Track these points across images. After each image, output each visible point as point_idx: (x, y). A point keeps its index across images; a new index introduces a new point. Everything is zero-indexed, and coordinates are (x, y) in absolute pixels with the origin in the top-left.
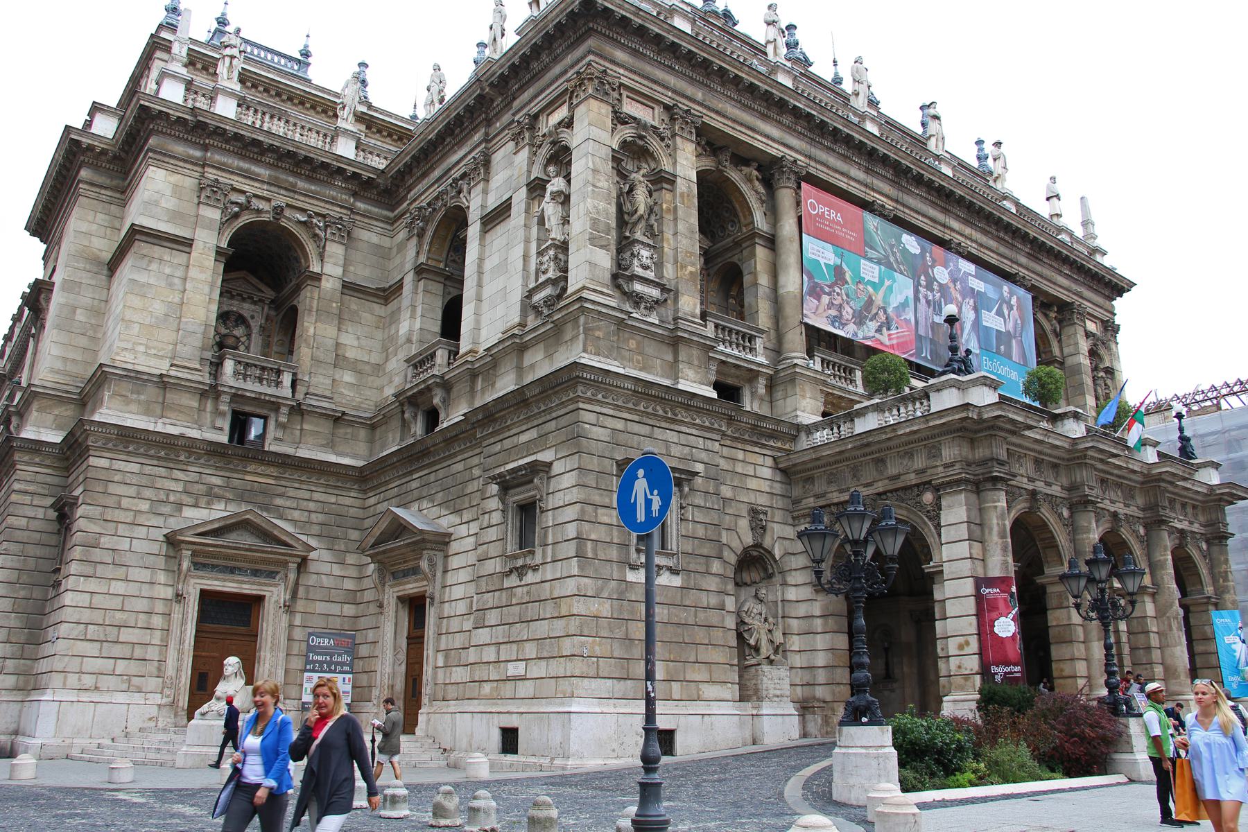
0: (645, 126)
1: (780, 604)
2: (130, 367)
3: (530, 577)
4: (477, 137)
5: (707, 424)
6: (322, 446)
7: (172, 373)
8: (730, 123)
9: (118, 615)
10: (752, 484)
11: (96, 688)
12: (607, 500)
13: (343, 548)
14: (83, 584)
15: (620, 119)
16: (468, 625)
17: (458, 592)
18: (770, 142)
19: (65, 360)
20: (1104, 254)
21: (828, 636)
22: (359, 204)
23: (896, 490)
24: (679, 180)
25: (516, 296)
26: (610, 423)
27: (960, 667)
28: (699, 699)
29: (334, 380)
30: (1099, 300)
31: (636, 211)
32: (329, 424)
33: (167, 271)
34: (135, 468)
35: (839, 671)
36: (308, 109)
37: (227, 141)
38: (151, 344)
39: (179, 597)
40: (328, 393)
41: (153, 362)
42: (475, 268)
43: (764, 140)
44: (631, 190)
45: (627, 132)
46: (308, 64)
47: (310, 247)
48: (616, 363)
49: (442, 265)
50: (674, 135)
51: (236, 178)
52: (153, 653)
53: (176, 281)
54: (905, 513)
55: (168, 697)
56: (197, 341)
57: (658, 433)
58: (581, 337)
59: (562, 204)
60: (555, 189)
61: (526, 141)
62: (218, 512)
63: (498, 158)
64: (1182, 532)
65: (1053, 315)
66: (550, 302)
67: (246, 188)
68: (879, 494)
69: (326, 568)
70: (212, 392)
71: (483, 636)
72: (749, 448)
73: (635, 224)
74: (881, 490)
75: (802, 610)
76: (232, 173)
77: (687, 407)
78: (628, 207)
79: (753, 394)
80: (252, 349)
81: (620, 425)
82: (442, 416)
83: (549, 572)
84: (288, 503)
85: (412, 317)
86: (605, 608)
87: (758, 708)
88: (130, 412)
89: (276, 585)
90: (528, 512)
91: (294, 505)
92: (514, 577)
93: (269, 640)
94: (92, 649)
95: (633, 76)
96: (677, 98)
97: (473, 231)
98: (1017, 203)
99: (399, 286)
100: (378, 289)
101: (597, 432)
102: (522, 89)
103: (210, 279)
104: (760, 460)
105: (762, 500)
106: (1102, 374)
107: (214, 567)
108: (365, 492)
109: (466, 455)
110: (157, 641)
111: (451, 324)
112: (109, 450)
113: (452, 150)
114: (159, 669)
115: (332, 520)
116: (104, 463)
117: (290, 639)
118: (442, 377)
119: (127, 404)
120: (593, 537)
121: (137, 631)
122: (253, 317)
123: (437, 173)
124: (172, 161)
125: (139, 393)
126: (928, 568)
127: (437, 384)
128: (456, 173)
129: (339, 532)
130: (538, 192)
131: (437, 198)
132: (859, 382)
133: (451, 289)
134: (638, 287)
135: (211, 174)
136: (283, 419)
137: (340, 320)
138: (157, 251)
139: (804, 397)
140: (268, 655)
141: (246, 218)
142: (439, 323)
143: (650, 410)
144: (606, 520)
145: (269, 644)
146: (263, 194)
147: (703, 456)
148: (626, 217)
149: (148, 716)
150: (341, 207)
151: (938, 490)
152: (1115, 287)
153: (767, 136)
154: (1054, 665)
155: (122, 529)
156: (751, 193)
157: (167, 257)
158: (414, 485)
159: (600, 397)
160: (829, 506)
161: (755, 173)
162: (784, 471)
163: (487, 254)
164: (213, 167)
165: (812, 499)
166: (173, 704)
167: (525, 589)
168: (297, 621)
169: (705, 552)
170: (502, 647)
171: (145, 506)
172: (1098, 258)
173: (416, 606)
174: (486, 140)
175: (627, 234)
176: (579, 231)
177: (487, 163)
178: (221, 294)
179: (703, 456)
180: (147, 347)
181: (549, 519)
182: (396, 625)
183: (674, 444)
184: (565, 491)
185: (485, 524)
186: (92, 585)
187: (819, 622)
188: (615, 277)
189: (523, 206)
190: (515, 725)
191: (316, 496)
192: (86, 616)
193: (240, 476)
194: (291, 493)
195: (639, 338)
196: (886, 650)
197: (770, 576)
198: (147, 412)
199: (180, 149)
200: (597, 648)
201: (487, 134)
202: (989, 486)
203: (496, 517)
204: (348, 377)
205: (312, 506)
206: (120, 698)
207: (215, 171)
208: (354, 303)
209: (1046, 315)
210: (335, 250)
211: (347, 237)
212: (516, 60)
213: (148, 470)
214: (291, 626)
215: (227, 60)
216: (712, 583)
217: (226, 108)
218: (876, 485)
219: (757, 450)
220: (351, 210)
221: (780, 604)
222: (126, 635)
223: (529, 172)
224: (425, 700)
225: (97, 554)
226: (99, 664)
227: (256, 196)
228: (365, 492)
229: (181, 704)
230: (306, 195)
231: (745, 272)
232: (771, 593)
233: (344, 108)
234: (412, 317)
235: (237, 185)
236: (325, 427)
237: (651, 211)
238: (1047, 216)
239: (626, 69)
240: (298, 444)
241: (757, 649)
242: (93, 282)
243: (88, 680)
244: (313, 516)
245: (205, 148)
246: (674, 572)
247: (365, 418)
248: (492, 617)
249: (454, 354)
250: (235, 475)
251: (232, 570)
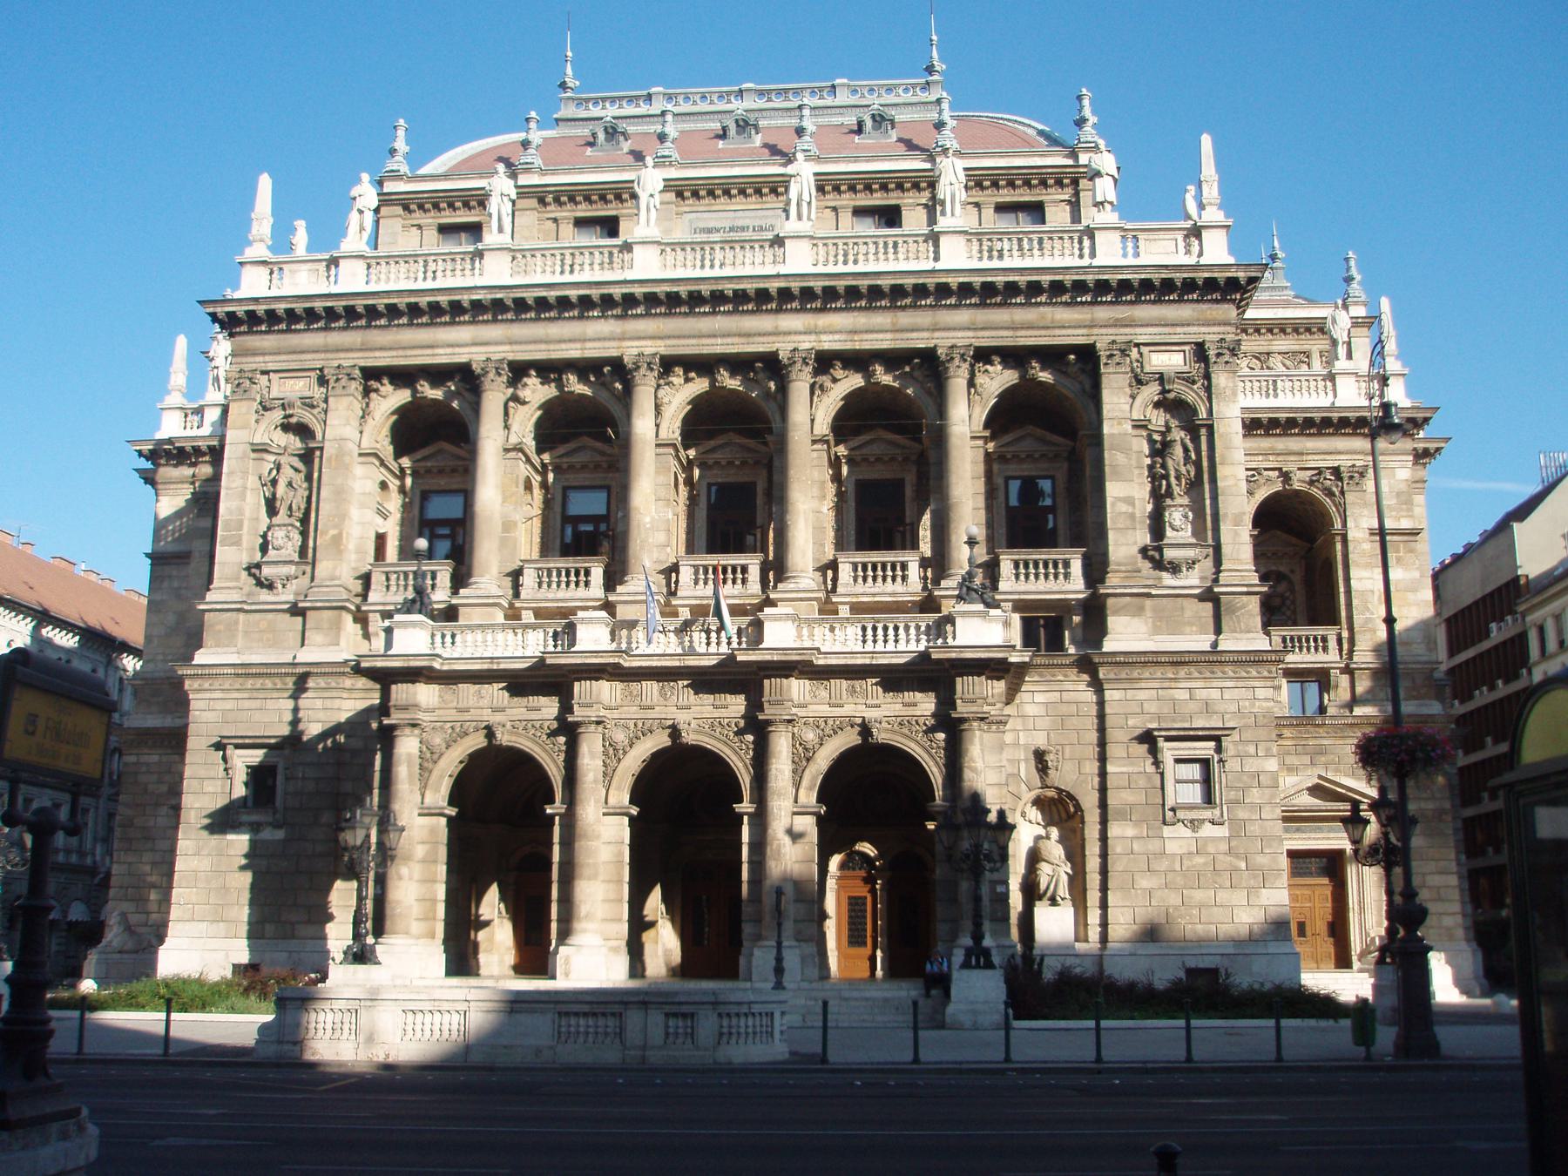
0: (292, 405)
5: (323, 685)
8: (401, 353)
12: (212, 774)
18: (457, 350)
24: (327, 445)
26: (220, 705)
28: (293, 937)
33: (176, 584)
34: (155, 758)
43: (449, 350)
57: (270, 704)
81: (229, 705)
86: (204, 864)
116: (132, 759)
134: (267, 571)
144: (210, 789)
157: (174, 573)
213: (164, 759)
246: (277, 826)
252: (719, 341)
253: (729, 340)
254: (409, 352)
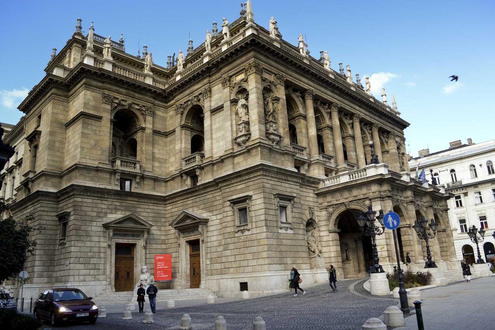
1: (318, 237)
2: (85, 164)
3: (247, 233)
4: (206, 81)
5: (296, 181)
6: (151, 189)
7: (100, 166)
9: (90, 254)
10: (308, 199)
11: (85, 281)
12: (272, 207)
13: (160, 225)
14: (77, 244)
15: (264, 80)
16: (221, 249)
17: (214, 238)
18: (305, 84)
19: (53, 161)
20: (399, 114)
21: (335, 247)
22: (157, 102)
23: (356, 200)
24: (281, 99)
25: (229, 139)
27: (381, 255)
29: (153, 166)
30: (399, 130)
31: (270, 111)
33: (94, 128)
35: (339, 258)
36: (128, 64)
37: (111, 80)
38: (91, 155)
39: (110, 246)
40: (151, 170)
41: (93, 162)
42: (209, 128)
43: (303, 84)
44: (267, 104)
45: (266, 84)
46: (123, 45)
47: (141, 118)
48: (270, 162)
49: (190, 125)
51: (115, 93)
52: (101, 267)
53: (97, 132)
54: (359, 207)
55: (109, 282)
56: (107, 154)
58: (260, 154)
59: (245, 108)
60: (243, 104)
61: (228, 85)
62: (119, 216)
63: (215, 89)
64: (435, 209)
65: (385, 136)
66: (244, 142)
67: (118, 97)
68: (350, 201)
69: (155, 232)
70: (113, 172)
71: (228, 253)
72: (307, 187)
73: (270, 116)
74: (351, 200)
75: (325, 239)
76: (113, 91)
77: (291, 176)
78: (267, 110)
80: (117, 154)
81: (273, 183)
82: (199, 179)
83: (254, 231)
84: (141, 210)
85: (181, 143)
86: (273, 242)
87: (317, 271)
88: (87, 181)
89: (140, 240)
90: (243, 211)
91: (143, 211)
93: (139, 259)
94: (81, 266)
95: (266, 65)
96: (278, 71)
97: (207, 114)
98: (374, 99)
99: (174, 131)
100: (164, 132)
101: (267, 186)
102: (225, 66)
103: (109, 131)
104: (310, 191)
105: (311, 204)
106: (401, 155)
107: (119, 234)
108: (166, 205)
109: (213, 192)
110: (102, 262)
112: (82, 195)
113: (194, 85)
114: (104, 272)
115: (156, 215)
116: (80, 200)
117: (146, 258)
118: (200, 165)
119: (85, 178)
120: (269, 219)
121: (95, 259)
122: (116, 142)
123: (187, 92)
124: (92, 88)
125: (89, 174)
127: (197, 168)
128: (196, 94)
129: (158, 219)
130: (234, 103)
131: (189, 101)
132: (333, 163)
133: (193, 133)
134: (272, 137)
135: (107, 92)
136: (138, 180)
137: (153, 144)
138: (90, 121)
139: (320, 169)
140: (139, 264)
141: (119, 108)
142: (190, 145)
143: (281, 177)
144: (272, 213)
145: (139, 261)
146: (124, 99)
147: (295, 191)
148: (267, 113)
149: (103, 289)
150: (150, 103)
151: (371, 200)
152: (403, 125)
153: (304, 82)
154: (404, 253)
155: (88, 223)
157: (93, 123)
158: (189, 202)
159: (267, 174)
160: (333, 205)
161: (300, 94)
162: (316, 194)
163: (213, 123)
164: (107, 89)
165: (326, 203)
166: (110, 284)
167: (245, 237)
168: (147, 252)
169: (298, 222)
170: (237, 256)
171: (95, 214)
172: (397, 115)
173: (194, 245)
175: (268, 119)
176: (254, 119)
177: (210, 91)
178: (113, 136)
179: (295, 191)
180: (90, 157)
181: (253, 214)
182: (186, 250)
183: (289, 188)
184: (258, 205)
185: (225, 215)
186: (80, 244)
187: (331, 242)
188: (266, 134)
189: (229, 108)
190: (246, 281)
191: (150, 207)
192: (79, 255)
193: (125, 202)
194: (142, 206)
195: (274, 153)
196: (346, 251)
197: (315, 228)
198: (92, 180)
199: (94, 83)
200: (273, 255)
201: (209, 81)
202: (387, 199)
203: (230, 213)
204: (157, 164)
205: (149, 211)
206: (92, 283)
207: (107, 91)
208: (157, 138)
209: (383, 136)
210: (149, 118)
211: (153, 114)
212: (224, 56)
213: (95, 201)
214: (146, 253)
215: (107, 49)
216: (301, 232)
217: (108, 67)
218: (349, 199)
219: (309, 188)
220: (153, 104)
221: (318, 237)
222: (93, 261)
223: (230, 96)
224: (203, 275)
225: (81, 233)
226: (85, 272)
227: (122, 100)
229: (112, 284)
230: (138, 99)
231: (297, 128)
232: (316, 234)
233: (147, 66)
234: (181, 143)
235: (116, 96)
236: (151, 182)
237: (274, 111)
238: (382, 102)
239: (264, 62)
240: (143, 189)
241: (314, 252)
242: (60, 132)
243: (82, 278)
244: (150, 215)
245: (103, 82)
246: (292, 229)
247: (164, 179)
248: (231, 246)
250: (124, 201)
251: (125, 235)
252: (347, 106)
253: (349, 107)
254: (296, 80)
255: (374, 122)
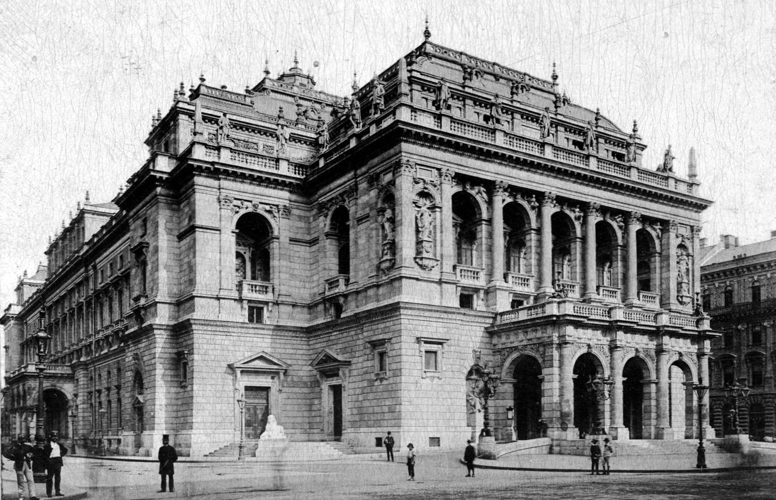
3: (385, 382)
32: (291, 307)
50: (441, 183)
79: (478, 297)
92: (379, 381)
111: (344, 266)
126: (540, 377)
148: (420, 229)
156: (481, 197)
174: (356, 176)
177: (357, 190)
201: (355, 174)
228: (309, 338)
249: (347, 281)
255: (630, 210)
